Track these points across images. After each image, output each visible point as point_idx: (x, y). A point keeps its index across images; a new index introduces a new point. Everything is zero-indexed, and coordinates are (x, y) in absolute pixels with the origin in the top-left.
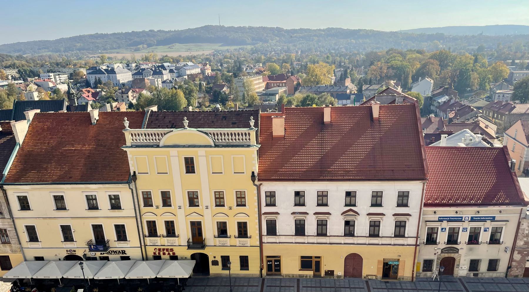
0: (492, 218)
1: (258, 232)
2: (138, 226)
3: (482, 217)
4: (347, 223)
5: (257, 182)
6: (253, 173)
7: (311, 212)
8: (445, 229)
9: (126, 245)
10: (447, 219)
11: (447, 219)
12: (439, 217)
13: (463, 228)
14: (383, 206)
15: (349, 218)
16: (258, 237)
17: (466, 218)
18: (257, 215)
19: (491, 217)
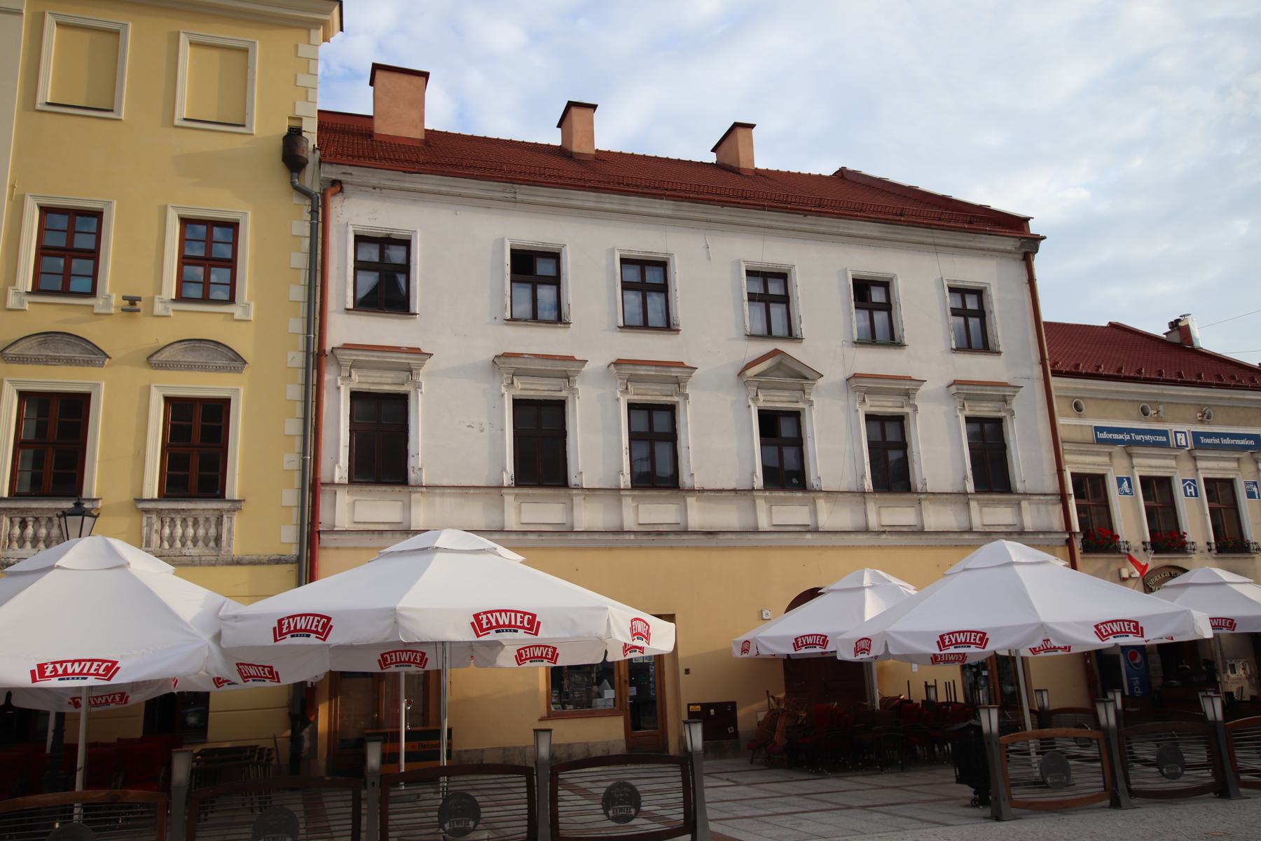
0: (1252, 443)
1: (291, 460)
3: (1225, 435)
4: (770, 422)
5: (311, 179)
7: (597, 361)
8: (1128, 479)
10: (1121, 437)
11: (1121, 437)
12: (1098, 429)
13: (1184, 481)
14: (906, 343)
15: (779, 401)
16: (290, 497)
17: (1178, 435)
18: (296, 359)
19: (1249, 437)
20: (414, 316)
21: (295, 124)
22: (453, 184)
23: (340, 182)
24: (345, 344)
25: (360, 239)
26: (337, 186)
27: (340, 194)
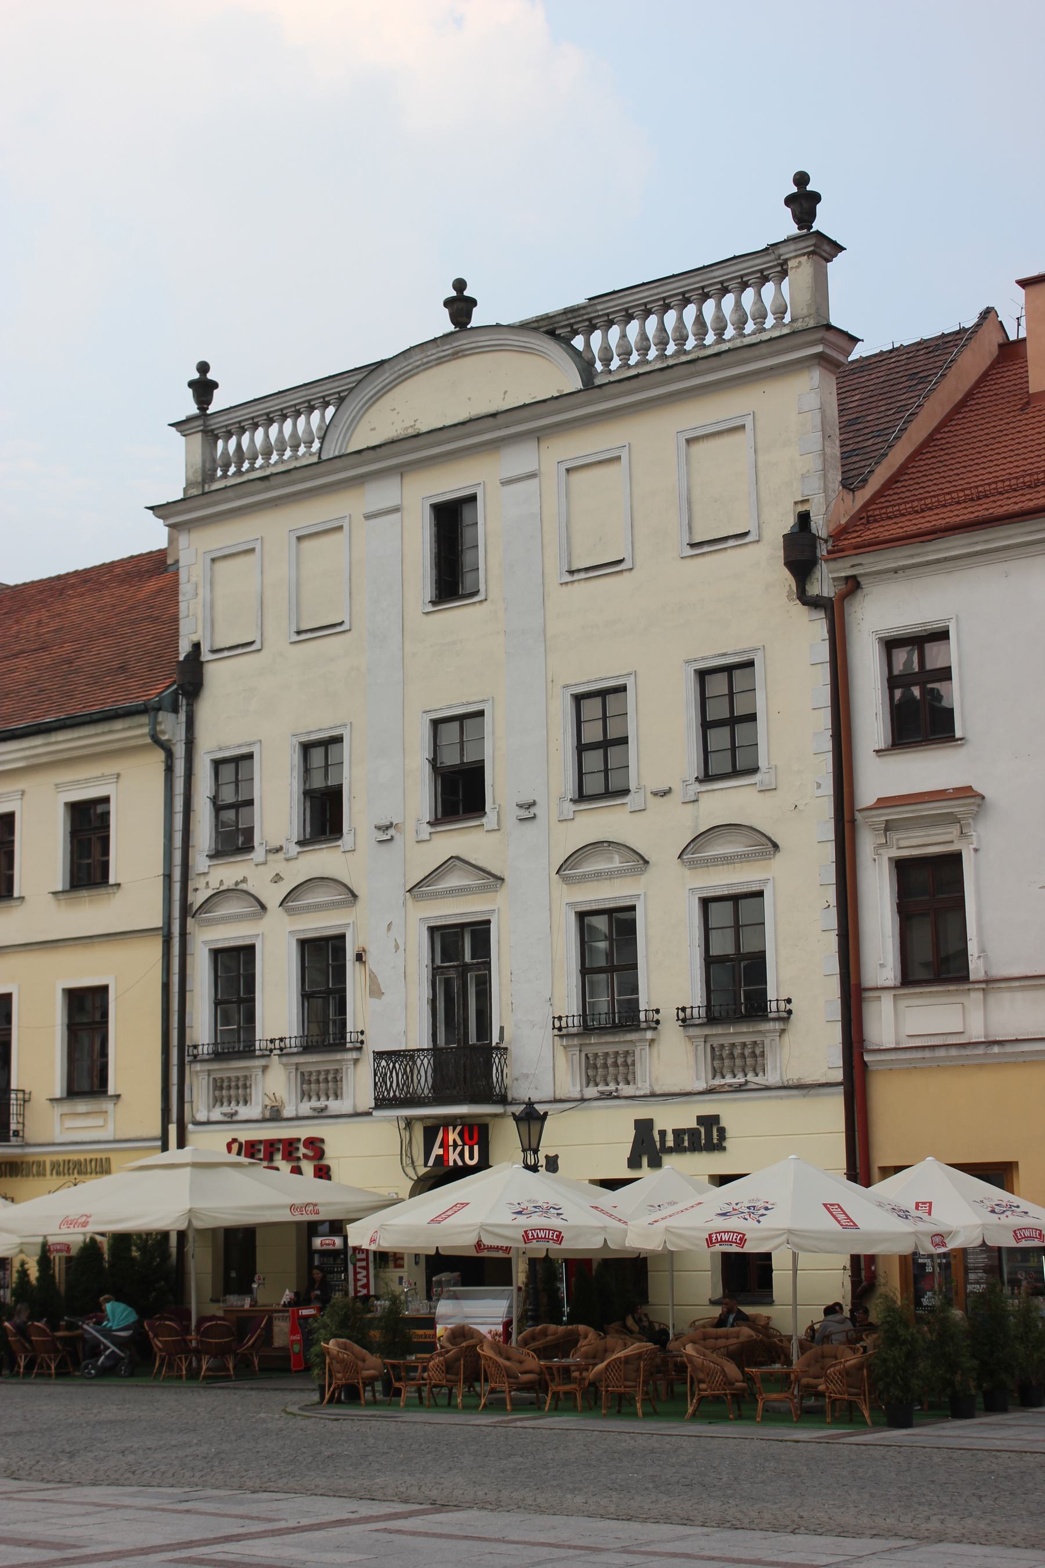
2: (166, 987)
5: (823, 584)
6: (804, 519)
9: (100, 1122)
20: (959, 742)
21: (801, 508)
22: (986, 537)
23: (854, 578)
24: (879, 800)
25: (891, 645)
26: (853, 585)
27: (859, 591)
